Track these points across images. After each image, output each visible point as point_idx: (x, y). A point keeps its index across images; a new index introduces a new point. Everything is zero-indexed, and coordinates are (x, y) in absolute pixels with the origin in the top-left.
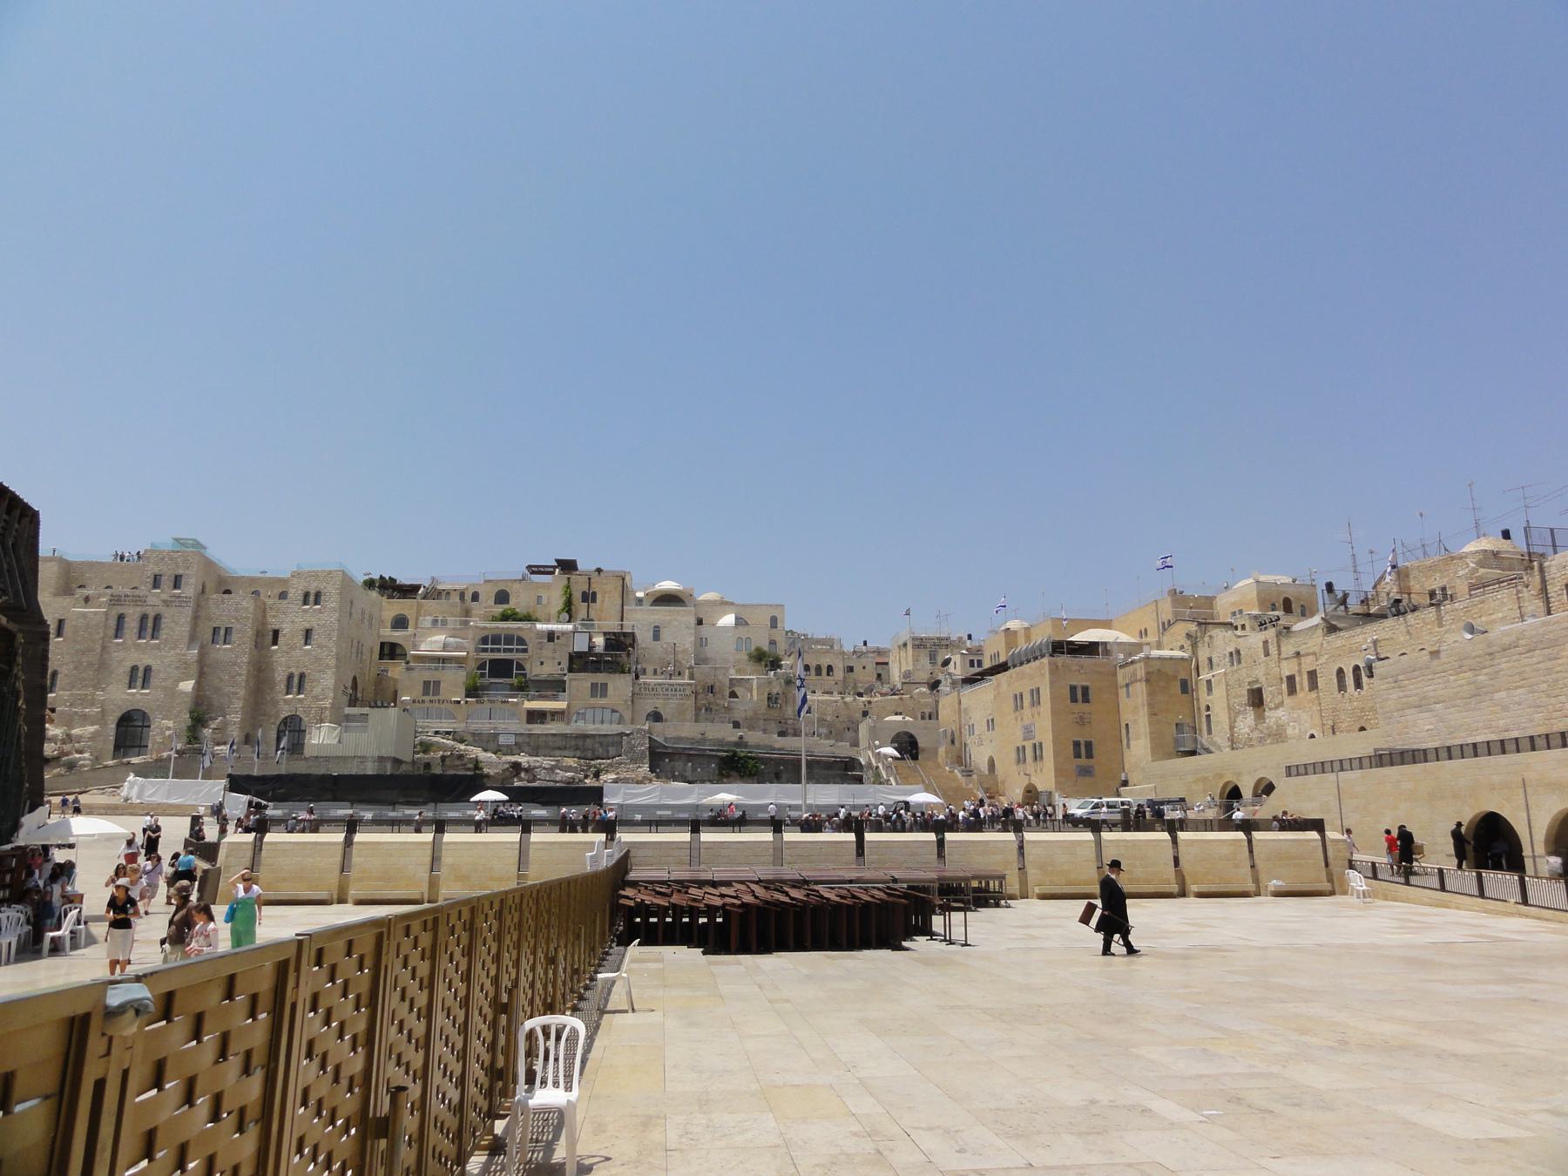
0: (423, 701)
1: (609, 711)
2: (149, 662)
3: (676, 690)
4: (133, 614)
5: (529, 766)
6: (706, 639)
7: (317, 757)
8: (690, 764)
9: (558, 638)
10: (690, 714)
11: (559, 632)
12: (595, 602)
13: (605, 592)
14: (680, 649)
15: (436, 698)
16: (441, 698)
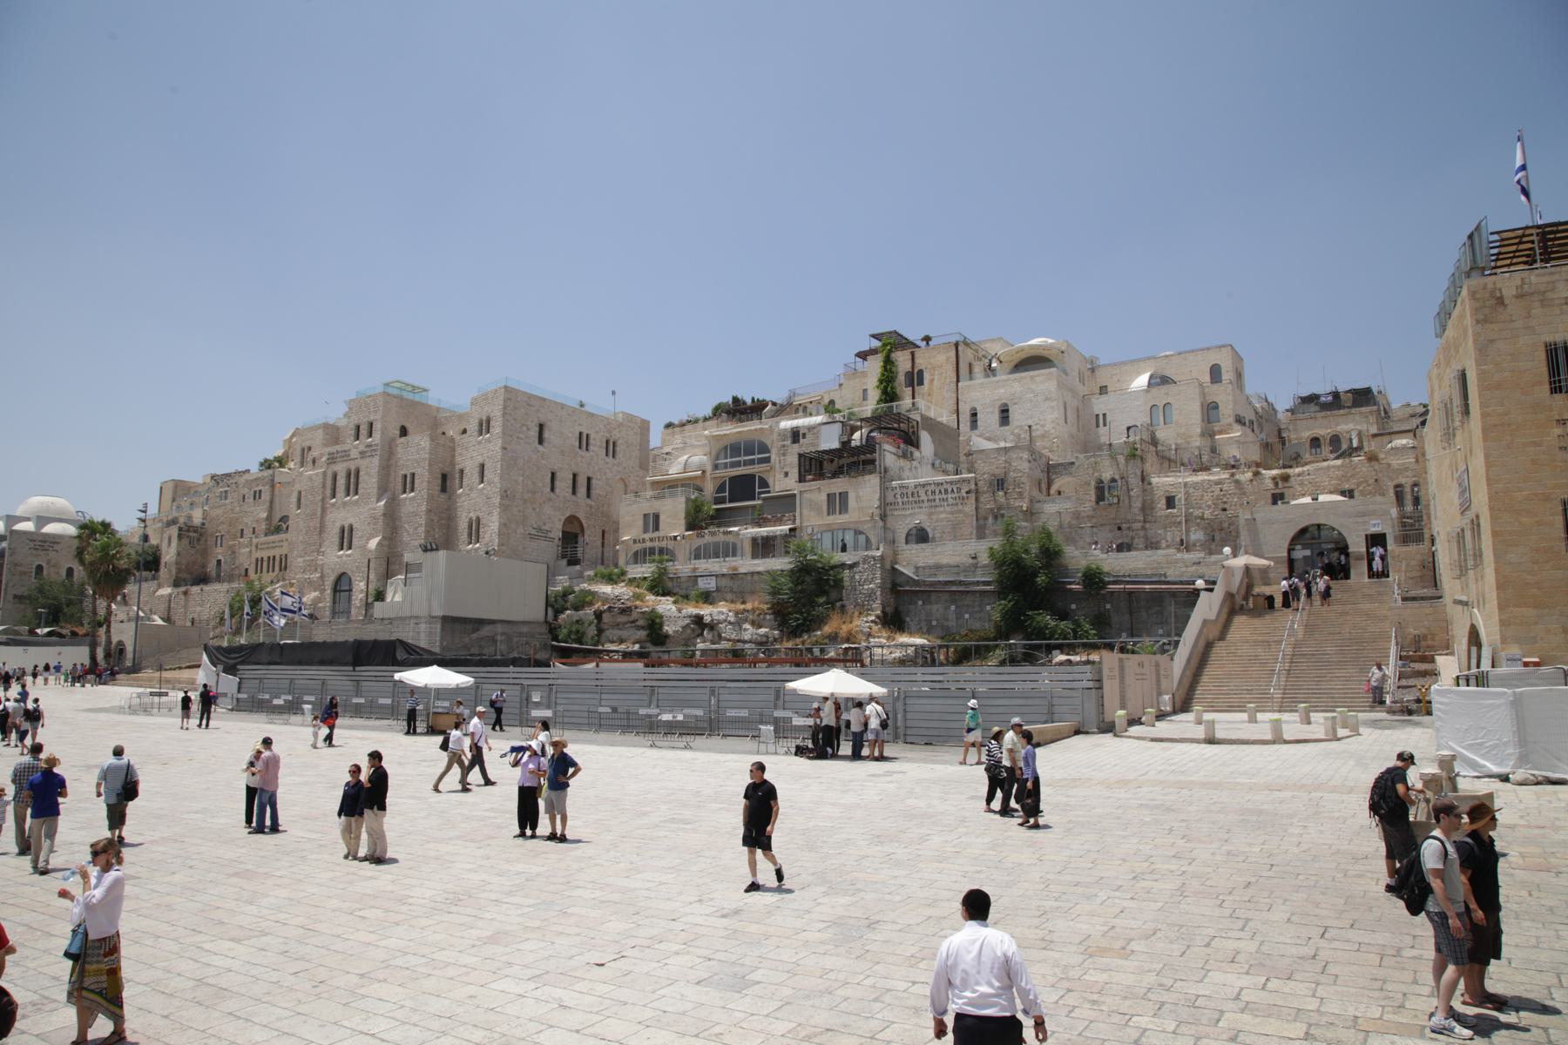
0: (644, 540)
1: (852, 533)
2: (351, 520)
3: (946, 491)
4: (341, 468)
5: (712, 620)
6: (1104, 415)
7: (382, 619)
8: (953, 608)
9: (804, 435)
10: (970, 526)
11: (804, 427)
12: (922, 384)
13: (934, 368)
14: (1038, 433)
15: (656, 534)
16: (661, 533)
